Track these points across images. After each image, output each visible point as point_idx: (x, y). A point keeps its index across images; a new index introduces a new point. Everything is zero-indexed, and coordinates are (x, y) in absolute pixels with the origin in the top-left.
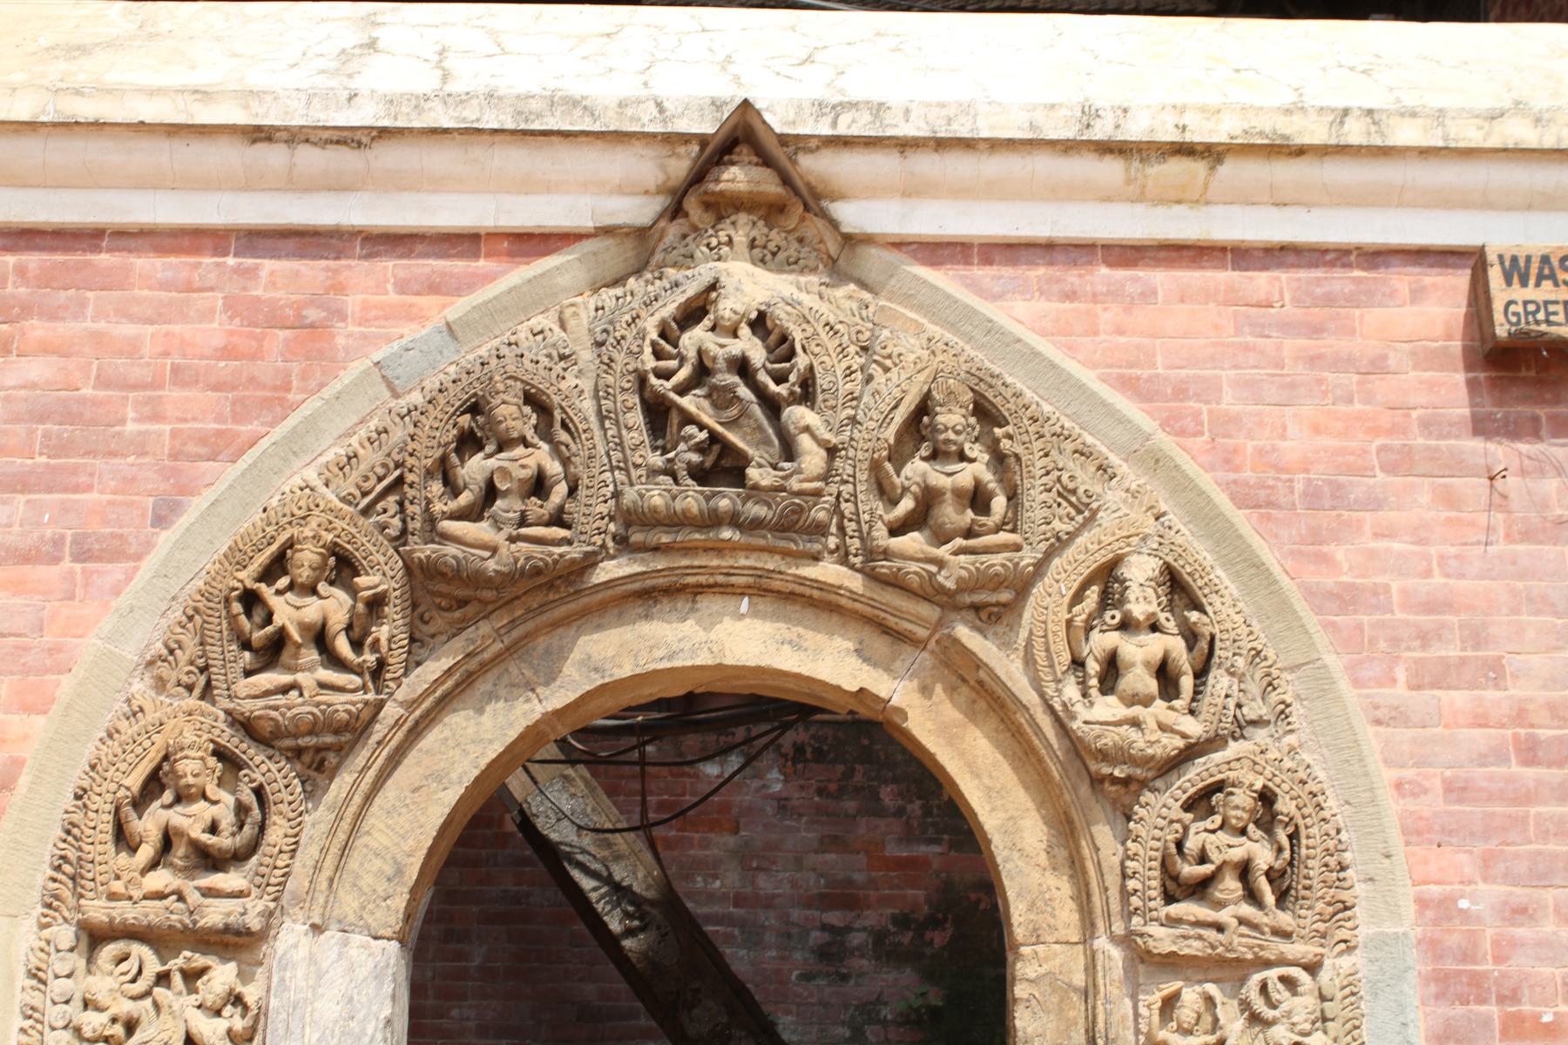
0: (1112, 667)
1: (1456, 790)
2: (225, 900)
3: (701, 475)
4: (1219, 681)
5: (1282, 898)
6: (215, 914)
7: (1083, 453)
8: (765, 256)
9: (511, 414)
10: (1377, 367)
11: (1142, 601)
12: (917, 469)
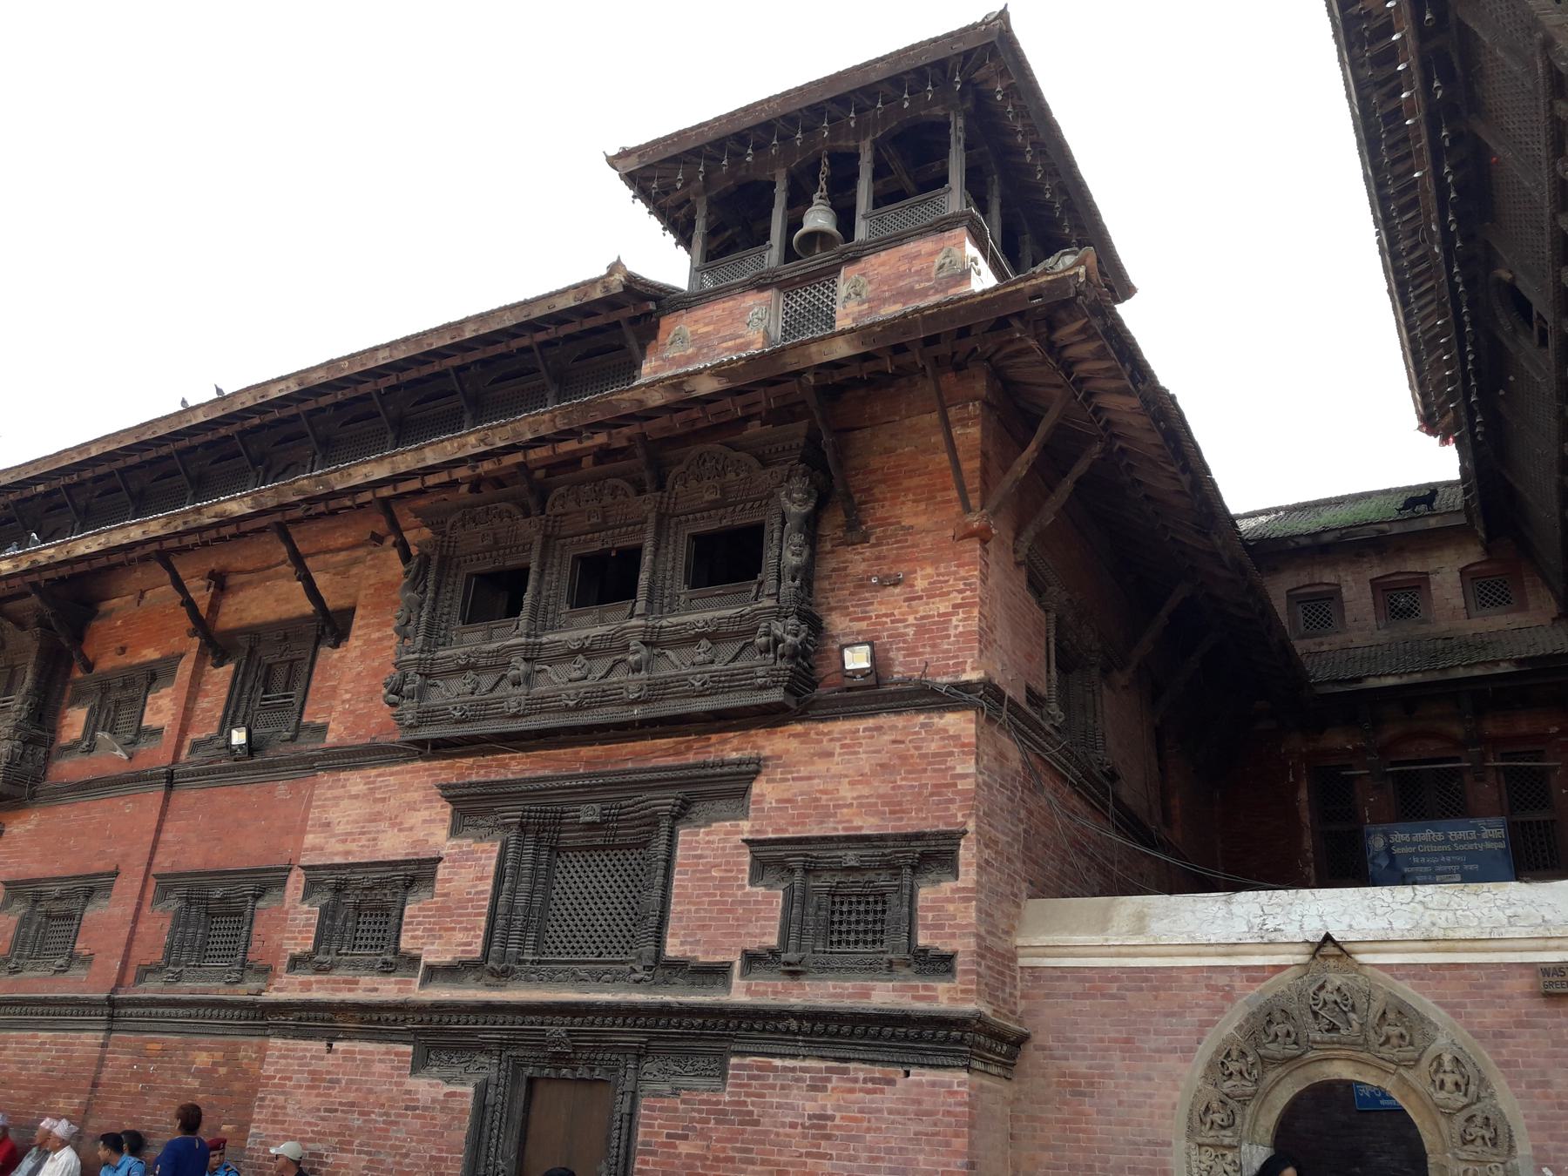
0: (1442, 1083)
1: (1541, 1117)
2: (1227, 1137)
3: (1328, 1031)
4: (1472, 1088)
5: (1494, 1145)
6: (1227, 1141)
7: (1431, 1023)
8: (1338, 970)
9: (1278, 1016)
10: (1512, 997)
11: (1448, 1066)
12: (1386, 1028)
